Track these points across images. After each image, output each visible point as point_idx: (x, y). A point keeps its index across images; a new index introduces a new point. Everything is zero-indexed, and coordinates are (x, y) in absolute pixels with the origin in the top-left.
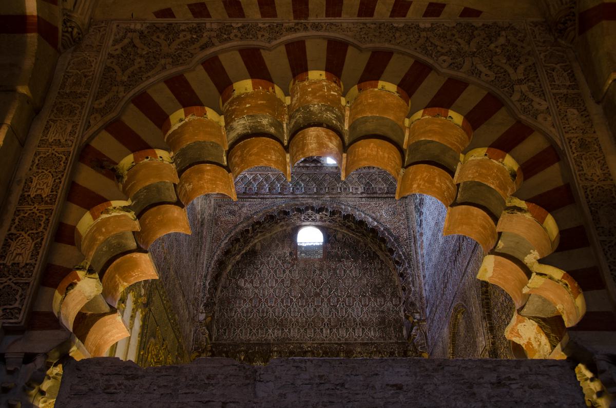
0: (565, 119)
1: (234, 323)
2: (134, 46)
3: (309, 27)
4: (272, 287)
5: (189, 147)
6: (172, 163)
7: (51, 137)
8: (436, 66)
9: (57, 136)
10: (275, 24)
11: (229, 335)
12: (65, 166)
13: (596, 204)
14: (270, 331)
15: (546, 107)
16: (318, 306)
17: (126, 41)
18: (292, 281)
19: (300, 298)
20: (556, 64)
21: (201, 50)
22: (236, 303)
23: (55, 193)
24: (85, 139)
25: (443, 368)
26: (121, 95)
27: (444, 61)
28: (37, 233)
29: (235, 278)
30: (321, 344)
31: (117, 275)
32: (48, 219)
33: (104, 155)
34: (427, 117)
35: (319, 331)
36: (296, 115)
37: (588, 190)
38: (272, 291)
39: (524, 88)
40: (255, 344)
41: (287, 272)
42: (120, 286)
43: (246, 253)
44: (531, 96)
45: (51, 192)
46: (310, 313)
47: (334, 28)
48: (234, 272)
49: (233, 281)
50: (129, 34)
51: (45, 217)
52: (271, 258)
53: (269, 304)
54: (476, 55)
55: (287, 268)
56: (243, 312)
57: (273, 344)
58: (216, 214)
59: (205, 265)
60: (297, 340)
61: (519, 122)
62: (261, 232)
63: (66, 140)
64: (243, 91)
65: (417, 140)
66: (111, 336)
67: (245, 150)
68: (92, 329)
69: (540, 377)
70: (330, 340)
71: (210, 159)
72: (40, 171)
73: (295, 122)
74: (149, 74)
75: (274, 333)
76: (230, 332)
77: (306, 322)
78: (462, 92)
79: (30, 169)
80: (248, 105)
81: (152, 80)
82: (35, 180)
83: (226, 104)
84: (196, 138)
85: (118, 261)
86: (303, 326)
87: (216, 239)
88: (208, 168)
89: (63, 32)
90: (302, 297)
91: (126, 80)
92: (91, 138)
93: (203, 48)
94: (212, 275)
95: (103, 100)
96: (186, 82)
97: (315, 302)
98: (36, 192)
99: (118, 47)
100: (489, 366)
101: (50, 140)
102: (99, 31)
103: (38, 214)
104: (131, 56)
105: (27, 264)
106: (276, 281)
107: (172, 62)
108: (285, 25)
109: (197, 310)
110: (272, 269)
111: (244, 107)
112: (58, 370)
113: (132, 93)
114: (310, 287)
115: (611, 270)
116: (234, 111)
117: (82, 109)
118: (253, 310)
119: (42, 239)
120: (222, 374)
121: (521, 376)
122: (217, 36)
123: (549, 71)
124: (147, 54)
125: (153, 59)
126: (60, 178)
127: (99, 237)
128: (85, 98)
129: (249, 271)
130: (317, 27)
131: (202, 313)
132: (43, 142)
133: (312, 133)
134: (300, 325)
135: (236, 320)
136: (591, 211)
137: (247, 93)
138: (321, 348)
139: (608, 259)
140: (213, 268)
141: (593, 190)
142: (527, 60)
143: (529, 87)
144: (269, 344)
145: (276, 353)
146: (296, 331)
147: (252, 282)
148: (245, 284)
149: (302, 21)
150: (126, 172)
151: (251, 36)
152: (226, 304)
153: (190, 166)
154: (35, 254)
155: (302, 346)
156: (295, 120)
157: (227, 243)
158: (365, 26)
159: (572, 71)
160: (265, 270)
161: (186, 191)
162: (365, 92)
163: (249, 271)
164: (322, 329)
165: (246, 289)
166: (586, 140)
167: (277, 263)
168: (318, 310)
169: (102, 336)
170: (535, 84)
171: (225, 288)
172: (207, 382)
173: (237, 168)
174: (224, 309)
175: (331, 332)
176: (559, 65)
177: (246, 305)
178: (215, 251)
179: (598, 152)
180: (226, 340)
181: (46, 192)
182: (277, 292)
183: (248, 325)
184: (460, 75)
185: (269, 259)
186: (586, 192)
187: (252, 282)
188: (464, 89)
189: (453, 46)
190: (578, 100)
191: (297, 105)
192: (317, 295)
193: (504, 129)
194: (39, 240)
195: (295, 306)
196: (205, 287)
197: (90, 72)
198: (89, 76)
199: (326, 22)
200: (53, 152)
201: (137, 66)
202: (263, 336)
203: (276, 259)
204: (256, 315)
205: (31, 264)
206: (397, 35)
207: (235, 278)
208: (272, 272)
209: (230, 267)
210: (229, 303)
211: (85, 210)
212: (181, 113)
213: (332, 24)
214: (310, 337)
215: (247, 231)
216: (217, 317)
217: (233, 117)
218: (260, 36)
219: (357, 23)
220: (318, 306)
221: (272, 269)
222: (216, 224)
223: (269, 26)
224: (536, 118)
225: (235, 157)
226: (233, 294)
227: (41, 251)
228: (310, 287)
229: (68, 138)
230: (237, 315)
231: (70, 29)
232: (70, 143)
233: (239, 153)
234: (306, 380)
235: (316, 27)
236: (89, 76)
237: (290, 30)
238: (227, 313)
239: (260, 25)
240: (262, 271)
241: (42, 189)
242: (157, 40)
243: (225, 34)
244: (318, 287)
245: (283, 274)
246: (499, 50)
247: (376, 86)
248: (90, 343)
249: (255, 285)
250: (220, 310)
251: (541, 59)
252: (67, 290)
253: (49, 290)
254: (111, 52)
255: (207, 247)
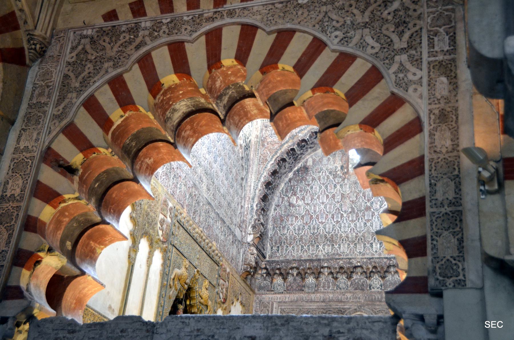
0: (433, 89)
1: (287, 240)
2: (86, 52)
3: (225, 15)
4: (323, 203)
5: (139, 132)
6: (113, 156)
7: (22, 145)
8: (328, 43)
9: (26, 143)
10: (197, 16)
11: (282, 252)
12: (31, 169)
13: (437, 177)
14: (321, 247)
15: (420, 76)
16: (368, 220)
17: (80, 47)
18: (343, 196)
19: (351, 212)
20: (440, 27)
21: (136, 50)
22: (288, 221)
23: (23, 192)
24: (46, 144)
25: (289, 323)
26: (74, 100)
27: (336, 37)
28: (11, 226)
29: (287, 196)
30: (370, 259)
31: (91, 242)
32: (18, 215)
33: (60, 156)
34: (318, 94)
35: (369, 245)
36: (228, 92)
37: (434, 162)
38: (322, 206)
39: (404, 58)
40: (306, 261)
41: (338, 187)
42: (97, 249)
43: (298, 171)
44: (408, 66)
45: (22, 191)
46: (361, 227)
47: (246, 12)
48: (286, 189)
49: (286, 198)
50: (83, 41)
51: (16, 213)
52: (323, 173)
53: (320, 221)
54: (367, 25)
55: (338, 183)
56: (295, 229)
57: (323, 260)
58: (263, 136)
59: (252, 188)
60: (347, 255)
61: (393, 94)
62: (310, 148)
63: (33, 146)
64: (172, 83)
65: (320, 111)
66: (89, 290)
67: (194, 123)
68: (68, 289)
69: (365, 332)
70: (380, 254)
71: (160, 138)
72: (14, 174)
73: (229, 98)
74: (95, 79)
75: (324, 249)
76: (282, 249)
77: (356, 237)
78: (348, 67)
79: (8, 173)
80: (181, 92)
81: (97, 84)
82: (10, 181)
83: (158, 97)
84: (140, 127)
85: (89, 232)
86: (353, 241)
87: (263, 160)
88: (161, 145)
89: (29, 49)
90: (353, 211)
91: (78, 86)
92: (51, 142)
93: (138, 48)
94: (259, 197)
95: (61, 108)
96: (124, 82)
97: (366, 216)
98: (11, 192)
99: (74, 54)
100: (326, 322)
101: (22, 148)
102: (59, 41)
103: (12, 211)
104: (83, 62)
105: (3, 251)
106: (327, 196)
107: (114, 65)
108: (205, 15)
109: (245, 232)
110: (323, 184)
111: (178, 94)
112: (27, 326)
113: (82, 97)
114: (361, 200)
115: (433, 240)
116: (169, 99)
117: (45, 117)
118: (304, 227)
119: (13, 230)
120: (131, 329)
121: (349, 330)
122: (149, 34)
123: (431, 37)
124: (95, 59)
125: (99, 63)
126: (27, 180)
127: (65, 219)
128: (47, 107)
129: (301, 188)
130: (231, 14)
131: (250, 234)
132: (16, 150)
133: (249, 103)
134: (350, 240)
135: (288, 238)
136: (430, 184)
137: (176, 84)
138: (370, 263)
139: (432, 229)
140: (260, 190)
141: (438, 162)
142: (415, 25)
143: (410, 56)
144: (319, 260)
145: (326, 269)
146: (346, 246)
147: (303, 199)
148: (297, 201)
149: (219, 9)
150: (80, 166)
151: (176, 31)
152: (279, 222)
153: (146, 145)
154: (8, 243)
155: (351, 261)
156: (227, 96)
157: (273, 164)
158: (273, 7)
159: (455, 33)
160: (316, 187)
161: (148, 164)
162: (269, 74)
163: (301, 188)
164: (372, 244)
165: (299, 206)
166: (445, 110)
167: (328, 177)
168: (368, 224)
169: (80, 291)
170: (417, 52)
171: (278, 206)
172: (120, 334)
173: (191, 139)
174: (277, 227)
175: (381, 247)
176: (443, 27)
177: (298, 222)
178: (262, 172)
179: (453, 123)
180: (279, 257)
181: (18, 191)
182: (328, 208)
183: (300, 241)
184: (349, 49)
185: (321, 174)
186: (431, 165)
187: (303, 199)
188: (351, 64)
189: (349, 18)
190: (451, 66)
191: (223, 86)
192: (368, 208)
193: (376, 104)
194: (11, 231)
195: (345, 221)
196: (252, 209)
197: (51, 82)
198: (50, 86)
199: (239, 8)
200: (23, 157)
201: (87, 71)
202: (314, 252)
203: (327, 174)
204: (308, 232)
205: (6, 251)
206: (300, 13)
207: (287, 196)
208: (323, 187)
209: (283, 185)
210: (282, 221)
211: (45, 204)
212: (120, 111)
213: (244, 8)
214: (360, 253)
215: (293, 150)
216: (271, 235)
217: (171, 103)
218: (183, 30)
219: (266, 4)
220: (368, 220)
221: (323, 184)
222: (263, 145)
223: (192, 18)
224: (407, 91)
225: (186, 131)
226: (285, 212)
227: (12, 240)
228: (361, 200)
229: (34, 145)
230: (290, 232)
231: (33, 47)
232: (34, 148)
233: (189, 127)
234: (188, 332)
235: (231, 13)
236: (50, 86)
237: (212, 19)
238: (280, 230)
239: (185, 18)
240: (314, 187)
241: (15, 190)
242: (104, 44)
243: (156, 31)
244: (368, 200)
245: (334, 189)
246: (390, 17)
247: (277, 68)
248: (69, 299)
249: (306, 202)
250: (274, 228)
251: (428, 23)
252: (35, 265)
253: (16, 269)
254: (68, 60)
255: (255, 169)
